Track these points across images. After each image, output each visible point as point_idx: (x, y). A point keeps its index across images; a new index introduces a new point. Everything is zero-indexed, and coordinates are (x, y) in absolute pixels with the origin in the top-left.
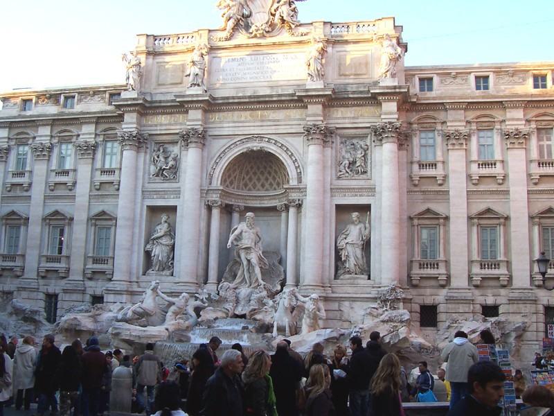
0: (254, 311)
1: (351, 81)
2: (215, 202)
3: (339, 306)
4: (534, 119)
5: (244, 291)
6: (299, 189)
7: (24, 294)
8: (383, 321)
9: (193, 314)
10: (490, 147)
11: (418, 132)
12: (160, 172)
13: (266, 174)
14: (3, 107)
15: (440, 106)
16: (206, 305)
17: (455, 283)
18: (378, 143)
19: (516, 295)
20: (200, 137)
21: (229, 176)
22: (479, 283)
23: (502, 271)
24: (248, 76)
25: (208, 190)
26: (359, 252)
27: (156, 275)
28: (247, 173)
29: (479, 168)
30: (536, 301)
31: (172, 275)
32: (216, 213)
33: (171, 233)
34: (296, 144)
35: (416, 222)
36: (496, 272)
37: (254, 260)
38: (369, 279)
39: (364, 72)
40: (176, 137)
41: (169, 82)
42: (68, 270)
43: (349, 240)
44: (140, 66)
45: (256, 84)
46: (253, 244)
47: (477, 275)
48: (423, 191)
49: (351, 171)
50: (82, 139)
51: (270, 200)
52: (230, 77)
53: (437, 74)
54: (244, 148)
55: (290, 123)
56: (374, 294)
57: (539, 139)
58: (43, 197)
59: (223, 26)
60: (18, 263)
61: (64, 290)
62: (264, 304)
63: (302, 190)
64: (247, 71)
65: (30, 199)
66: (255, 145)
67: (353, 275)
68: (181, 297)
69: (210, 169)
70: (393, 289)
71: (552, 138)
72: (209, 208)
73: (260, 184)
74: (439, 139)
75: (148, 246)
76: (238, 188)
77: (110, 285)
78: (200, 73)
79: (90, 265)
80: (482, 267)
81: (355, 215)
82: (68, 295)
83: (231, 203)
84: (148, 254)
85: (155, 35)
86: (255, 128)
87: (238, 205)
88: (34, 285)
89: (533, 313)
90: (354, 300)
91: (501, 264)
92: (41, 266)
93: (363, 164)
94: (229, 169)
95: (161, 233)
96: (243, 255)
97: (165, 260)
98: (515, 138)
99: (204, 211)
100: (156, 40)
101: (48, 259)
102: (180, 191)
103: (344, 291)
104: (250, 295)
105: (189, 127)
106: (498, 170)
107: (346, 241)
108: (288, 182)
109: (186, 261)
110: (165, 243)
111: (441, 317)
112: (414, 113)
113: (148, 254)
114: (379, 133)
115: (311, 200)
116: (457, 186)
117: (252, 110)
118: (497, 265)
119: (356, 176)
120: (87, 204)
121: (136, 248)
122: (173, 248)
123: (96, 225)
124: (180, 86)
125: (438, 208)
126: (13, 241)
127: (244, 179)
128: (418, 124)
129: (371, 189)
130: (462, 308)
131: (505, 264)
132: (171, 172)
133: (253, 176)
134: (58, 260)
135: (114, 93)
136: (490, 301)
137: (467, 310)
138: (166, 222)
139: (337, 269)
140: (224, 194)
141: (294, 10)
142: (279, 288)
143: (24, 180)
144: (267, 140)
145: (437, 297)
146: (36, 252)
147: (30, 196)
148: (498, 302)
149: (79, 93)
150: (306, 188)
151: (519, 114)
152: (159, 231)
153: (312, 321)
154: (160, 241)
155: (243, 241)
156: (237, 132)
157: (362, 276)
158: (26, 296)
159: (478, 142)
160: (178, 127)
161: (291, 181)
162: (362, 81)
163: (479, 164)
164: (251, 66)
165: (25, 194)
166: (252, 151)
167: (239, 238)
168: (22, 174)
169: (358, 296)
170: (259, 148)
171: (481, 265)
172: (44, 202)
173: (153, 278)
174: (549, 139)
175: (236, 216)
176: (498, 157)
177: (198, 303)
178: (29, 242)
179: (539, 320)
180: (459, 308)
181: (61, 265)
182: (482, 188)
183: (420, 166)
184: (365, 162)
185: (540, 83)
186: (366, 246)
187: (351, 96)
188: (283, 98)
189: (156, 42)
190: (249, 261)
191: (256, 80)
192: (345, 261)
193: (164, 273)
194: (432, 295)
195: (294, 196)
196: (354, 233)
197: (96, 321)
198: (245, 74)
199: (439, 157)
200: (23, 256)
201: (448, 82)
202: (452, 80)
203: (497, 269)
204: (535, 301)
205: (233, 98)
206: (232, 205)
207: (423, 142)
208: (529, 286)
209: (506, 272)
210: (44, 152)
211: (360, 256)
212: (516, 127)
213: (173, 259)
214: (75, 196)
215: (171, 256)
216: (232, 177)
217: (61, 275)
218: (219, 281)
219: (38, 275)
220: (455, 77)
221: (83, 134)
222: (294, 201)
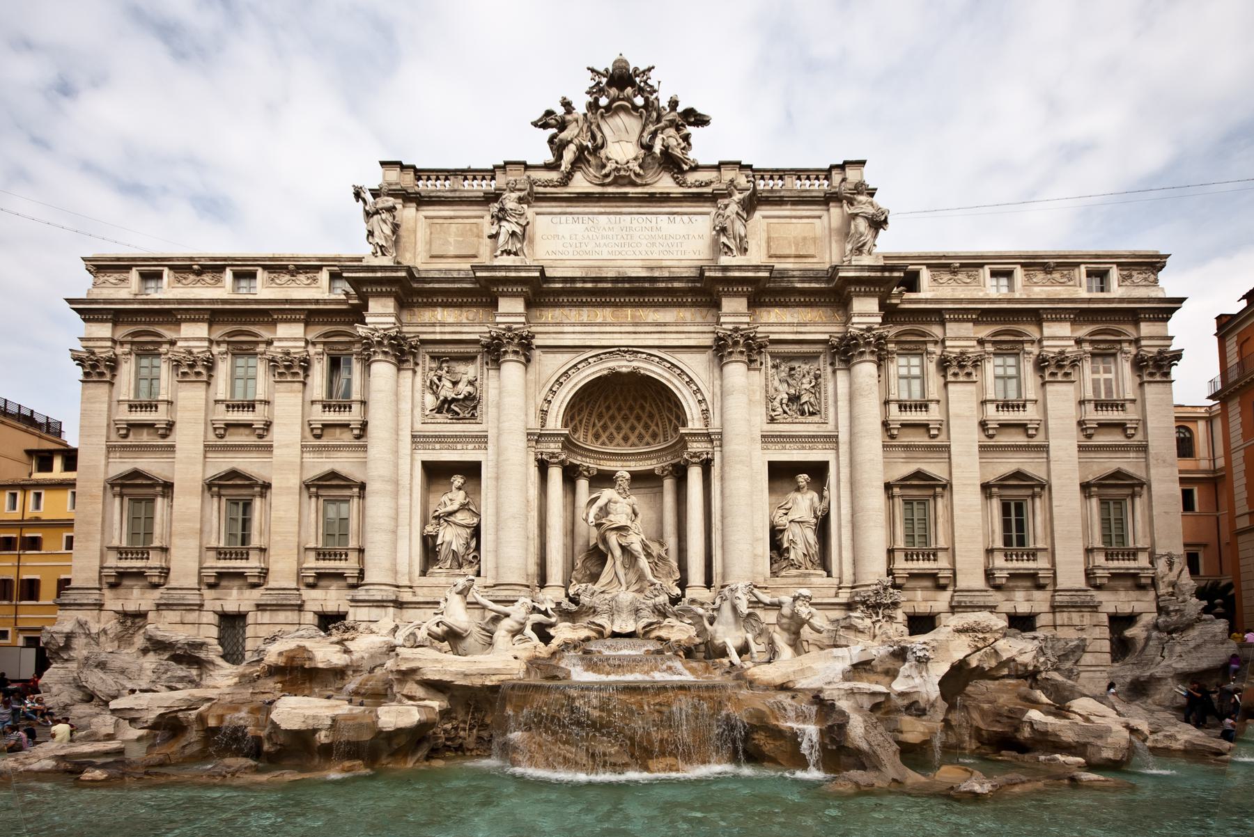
6: (708, 435)
23: (1042, 563)
24: (605, 250)
25: (540, 435)
26: (812, 537)
27: (448, 575)
30: (1096, 607)
34: (697, 365)
35: (896, 491)
37: (637, 547)
40: (471, 349)
41: (452, 253)
43: (794, 515)
45: (619, 263)
47: (1001, 569)
48: (907, 446)
50: (276, 349)
51: (641, 460)
52: (571, 250)
60: (155, 561)
61: (258, 605)
64: (602, 242)
65: (174, 451)
66: (623, 365)
67: (803, 570)
69: (540, 400)
72: (543, 467)
74: (932, 367)
77: (361, 594)
80: (1008, 558)
81: (803, 478)
86: (623, 336)
95: (455, 506)
96: (613, 539)
97: (462, 550)
101: (220, 554)
102: (486, 437)
108: (684, 424)
109: (509, 554)
116: (964, 438)
117: (615, 305)
119: (801, 419)
121: (403, 531)
122: (476, 532)
123: (317, 497)
126: (141, 527)
127: (594, 425)
128: (897, 343)
134: (244, 555)
138: (459, 489)
140: (569, 444)
142: (679, 592)
143: (159, 416)
146: (194, 543)
147: (173, 446)
152: (448, 503)
154: (452, 519)
158: (178, 619)
160: (477, 329)
164: (610, 233)
165: (161, 442)
171: (1006, 555)
172: (205, 457)
174: (1107, 371)
178: (176, 526)
181: (252, 564)
183: (900, 407)
186: (822, 527)
188: (676, 285)
191: (620, 257)
192: (787, 550)
195: (695, 447)
197: (347, 651)
199: (934, 391)
200: (165, 550)
205: (584, 280)
207: (904, 371)
209: (1049, 566)
210: (197, 369)
211: (812, 542)
213: (478, 548)
214: (271, 446)
215: (473, 544)
217: (251, 580)
219: (200, 582)
222: (695, 455)
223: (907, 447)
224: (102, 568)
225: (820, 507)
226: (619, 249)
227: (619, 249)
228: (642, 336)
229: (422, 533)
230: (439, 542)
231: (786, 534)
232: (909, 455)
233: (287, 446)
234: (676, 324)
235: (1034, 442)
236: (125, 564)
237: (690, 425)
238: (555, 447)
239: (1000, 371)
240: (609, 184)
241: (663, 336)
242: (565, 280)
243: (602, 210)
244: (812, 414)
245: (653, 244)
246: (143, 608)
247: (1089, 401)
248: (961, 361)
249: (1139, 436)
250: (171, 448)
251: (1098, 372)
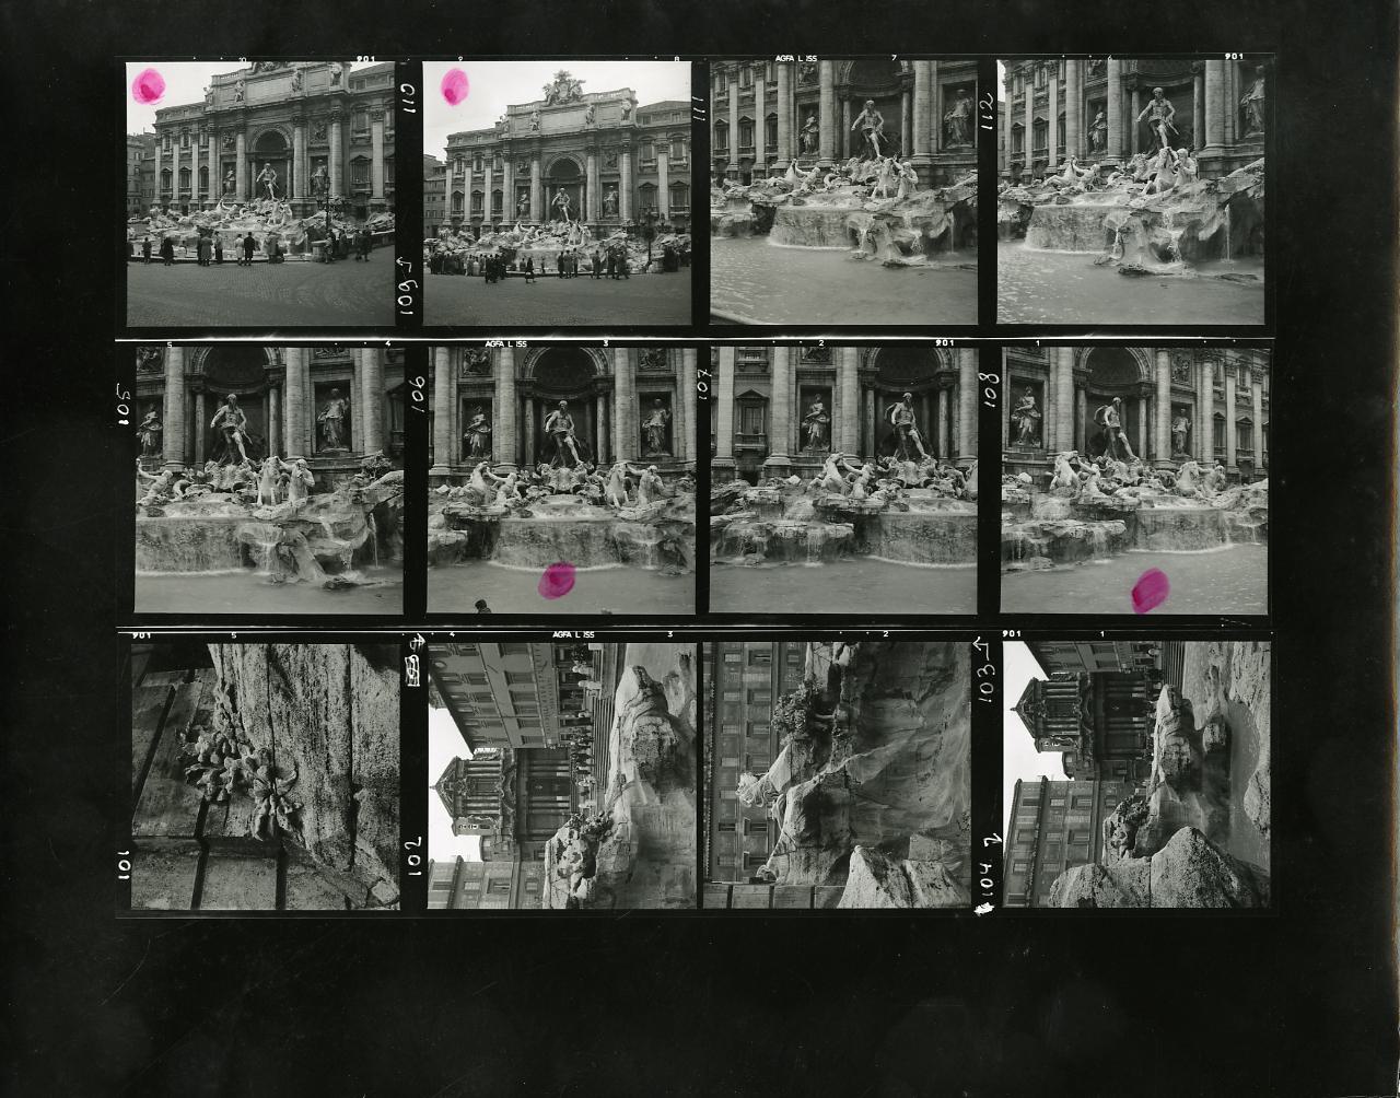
0: (564, 234)
20: (537, 155)
32: (548, 189)
33: (528, 198)
34: (582, 155)
84: (518, 208)
132: (527, 171)
141: (580, 89)
156: (559, 149)
181: (481, 215)
186: (617, 201)
248: (662, 146)
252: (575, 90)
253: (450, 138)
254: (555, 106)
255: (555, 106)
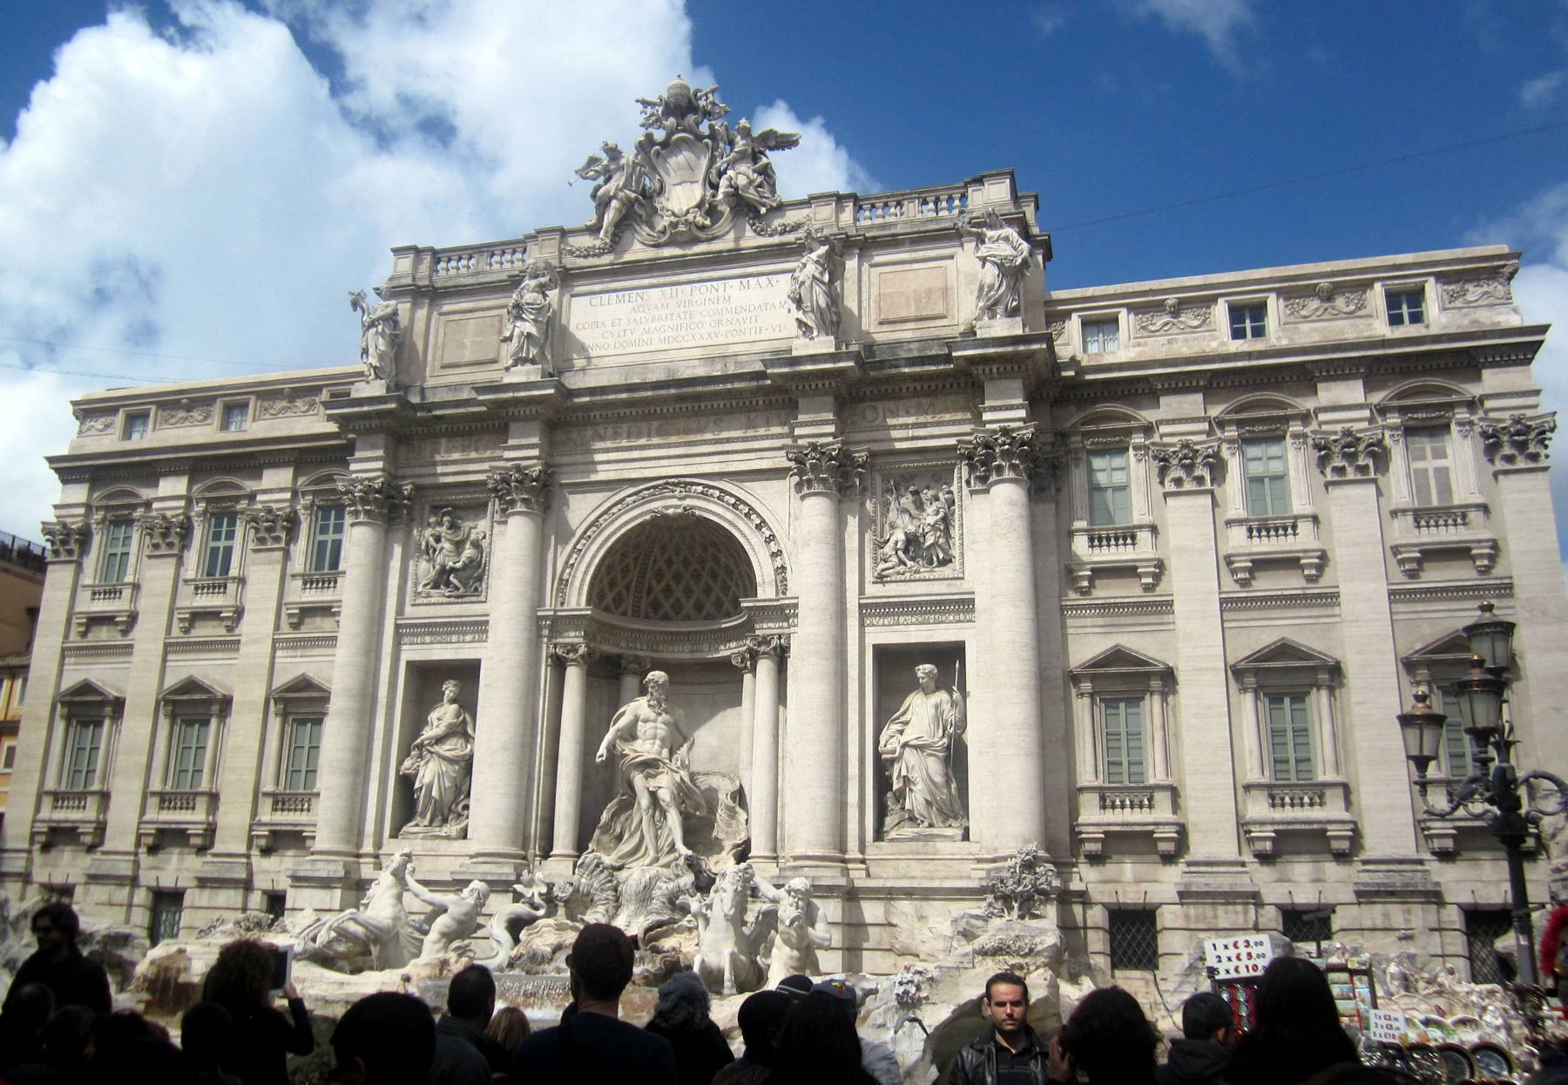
1: (908, 335)
2: (573, 648)
3: (887, 912)
4: (1395, 403)
5: (635, 875)
6: (782, 608)
7: (100, 892)
8: (983, 953)
9: (505, 937)
10: (1278, 483)
11: (1084, 456)
12: (442, 578)
13: (706, 578)
14: (80, 432)
15: (1140, 387)
16: (541, 912)
17: (1199, 848)
18: (979, 487)
19: (1379, 878)
21: (612, 584)
22: (1268, 845)
24: (655, 336)
28: (659, 576)
29: (1251, 537)
31: (465, 837)
32: (573, 676)
34: (774, 499)
36: (1316, 813)
37: (665, 795)
38: (966, 837)
39: (939, 310)
42: (210, 832)
44: (396, 323)
46: (665, 752)
47: (1262, 823)
49: (913, 559)
52: (611, 341)
53: (1131, 308)
54: (641, 515)
55: (757, 445)
56: (975, 877)
57: (1413, 455)
58: (161, 647)
59: (592, 219)
62: (685, 910)
63: (784, 612)
65: (131, 654)
66: (671, 505)
67: (923, 829)
68: (466, 891)
70: (1029, 865)
71: (1449, 451)
72: (559, 665)
73: (692, 601)
75: (408, 763)
76: (636, 614)
78: (534, 331)
79: (266, 815)
81: (924, 670)
82: (206, 893)
83: (616, 650)
84: (406, 783)
85: (437, 247)
87: (637, 657)
88: (125, 868)
89: (1432, 930)
90: (927, 894)
91: (1328, 793)
92: (147, 817)
93: (941, 541)
94: (610, 568)
96: (638, 780)
97: (449, 798)
98: (1349, 458)
99: (545, 673)
100: (439, 261)
103: (902, 872)
104: (648, 888)
105: (509, 464)
106: (1303, 540)
107: (903, 739)
110: (447, 754)
111: (1166, 942)
112: (1073, 408)
113: (406, 783)
114: (983, 462)
115: (808, 638)
116: (1194, 586)
118: (1319, 793)
120: (267, 661)
124: (495, 366)
125: (1142, 642)
127: (650, 590)
129: (963, 601)
130: (1226, 916)
131: (1340, 791)
133: (673, 584)
135: (332, 391)
136: (1305, 896)
137: (1240, 921)
138: (453, 701)
139: (881, 812)
140: (593, 629)
141: (766, 172)
144: (700, 489)
145: (1157, 887)
146: (138, 785)
148: (1328, 898)
149: (261, 396)
150: (796, 606)
151: (1352, 392)
153: (796, 953)
154: (436, 748)
155: (637, 745)
157: (949, 832)
158: (105, 898)
159: (1244, 469)
161: (759, 590)
162: (935, 333)
163: (1250, 530)
164: (663, 312)
166: (665, 517)
167: (630, 734)
168: (113, 593)
169: (936, 884)
170: (680, 511)
172: (165, 660)
173: (415, 839)
175: (630, 682)
176: (1299, 503)
177: (522, 908)
179: (1450, 950)
180: (1215, 917)
181: (195, 817)
182: (1266, 584)
183: (1091, 540)
184: (947, 534)
185: (1405, 310)
187: (907, 370)
188: (737, 385)
189: (442, 265)
190: (653, 795)
191: (675, 345)
193: (445, 830)
194: (1138, 881)
196: (921, 713)
198: (647, 331)
201: (1159, 323)
202: (1167, 319)
203: (1316, 808)
204: (1435, 897)
206: (620, 656)
208: (1411, 853)
211: (939, 779)
212: (1347, 425)
215: (465, 788)
216: (620, 587)
218: (581, 845)
220: (1176, 312)
221: (265, 492)
222: (765, 641)
223: (1105, 607)
224: (34, 821)
225: (950, 715)
226: (674, 334)
227: (674, 334)
228: (698, 460)
229: (398, 771)
230: (417, 785)
231: (896, 766)
232: (1109, 620)
233: (257, 641)
234: (744, 439)
235: (1314, 590)
236: (60, 815)
237: (761, 595)
238: (574, 637)
239: (1256, 469)
240: (666, 244)
241: (725, 458)
242: (592, 391)
243: (654, 281)
244: (945, 562)
245: (719, 322)
246: (71, 880)
247: (1404, 511)
249: (1498, 571)
250: (128, 649)
251: (1422, 457)
252: (742, 174)
253: (87, 411)
254: (637, 251)
255: (637, 251)
